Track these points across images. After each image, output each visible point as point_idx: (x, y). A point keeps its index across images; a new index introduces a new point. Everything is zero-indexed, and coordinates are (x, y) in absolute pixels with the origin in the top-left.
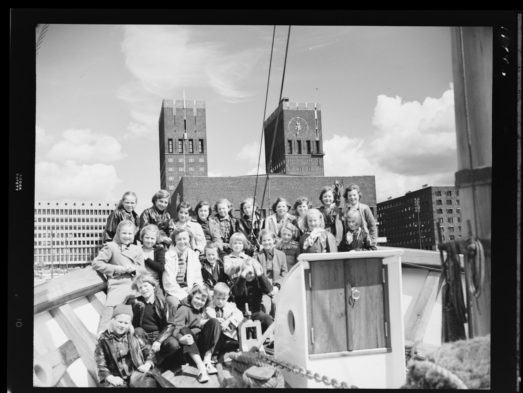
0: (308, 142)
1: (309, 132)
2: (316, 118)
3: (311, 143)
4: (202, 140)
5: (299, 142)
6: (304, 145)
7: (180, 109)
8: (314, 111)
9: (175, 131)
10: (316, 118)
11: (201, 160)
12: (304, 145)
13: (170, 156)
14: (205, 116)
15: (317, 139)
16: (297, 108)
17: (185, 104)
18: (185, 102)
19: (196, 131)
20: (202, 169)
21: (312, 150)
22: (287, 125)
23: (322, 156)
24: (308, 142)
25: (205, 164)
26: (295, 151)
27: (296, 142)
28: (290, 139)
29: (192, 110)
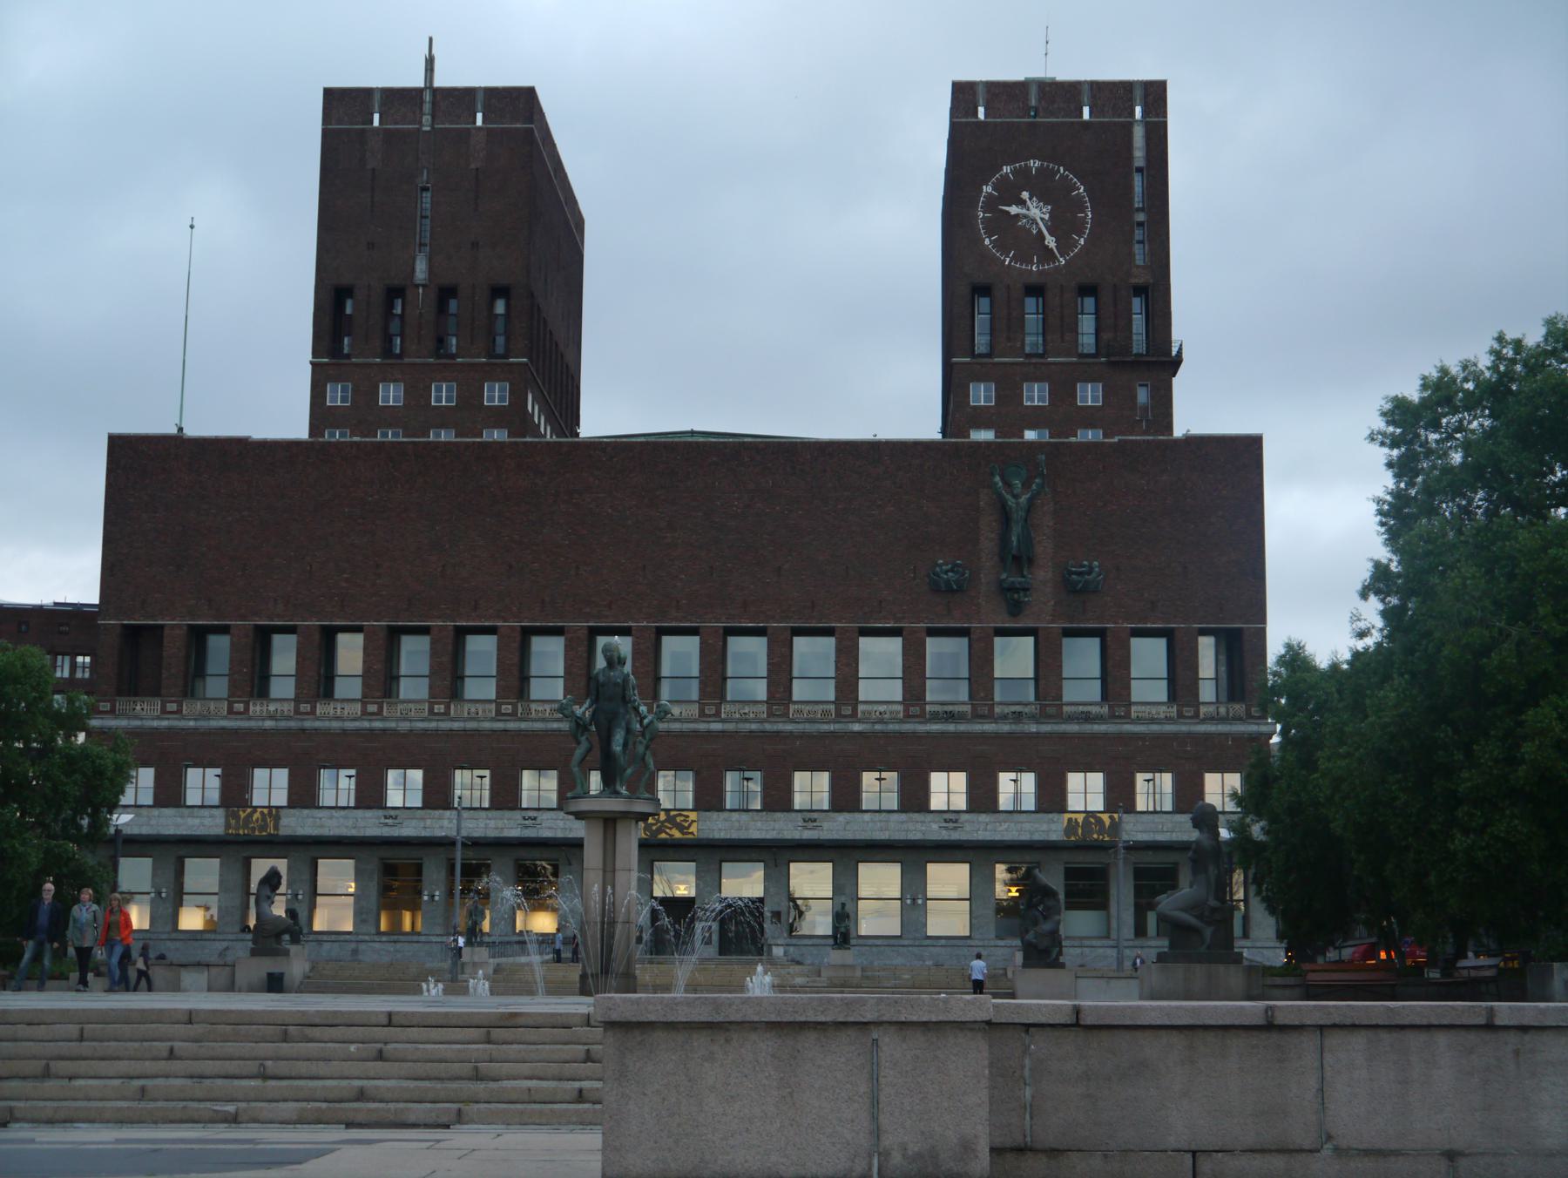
8: (1128, 128)
9: (371, 246)
15: (1139, 279)
17: (427, 107)
18: (427, 97)
19: (475, 245)
21: (1106, 336)
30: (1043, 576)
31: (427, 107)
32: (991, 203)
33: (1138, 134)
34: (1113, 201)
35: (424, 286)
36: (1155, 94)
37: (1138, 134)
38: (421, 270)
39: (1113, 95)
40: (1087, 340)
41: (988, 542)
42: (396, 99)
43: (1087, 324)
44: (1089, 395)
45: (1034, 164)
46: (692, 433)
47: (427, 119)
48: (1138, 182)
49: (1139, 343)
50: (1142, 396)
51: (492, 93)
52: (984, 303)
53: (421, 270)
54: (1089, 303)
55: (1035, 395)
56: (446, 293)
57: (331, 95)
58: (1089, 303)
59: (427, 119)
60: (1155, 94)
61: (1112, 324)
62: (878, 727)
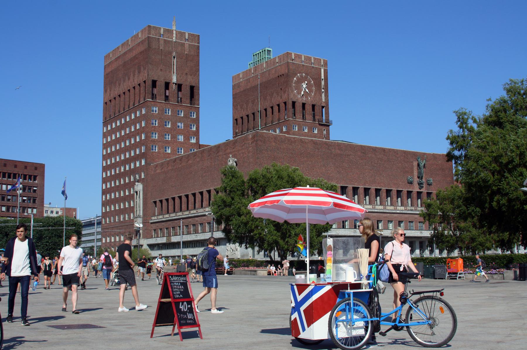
0: (313, 106)
1: (315, 94)
2: (323, 77)
3: (316, 108)
4: (192, 88)
5: (304, 105)
6: (308, 108)
7: (169, 41)
9: (161, 70)
10: (323, 77)
12: (308, 108)
13: (153, 103)
14: (198, 55)
17: (174, 35)
18: (174, 32)
21: (317, 117)
22: (292, 82)
23: (328, 126)
24: (313, 106)
25: (197, 121)
26: (299, 115)
27: (301, 105)
28: (294, 100)
29: (183, 45)
30: (424, 180)
31: (174, 35)
32: (296, 83)
33: (322, 71)
35: (176, 84)
37: (322, 71)
38: (174, 80)
41: (416, 173)
45: (304, 74)
47: (174, 38)
48: (323, 83)
50: (325, 132)
53: (174, 80)
56: (179, 87)
59: (174, 38)
62: (401, 212)
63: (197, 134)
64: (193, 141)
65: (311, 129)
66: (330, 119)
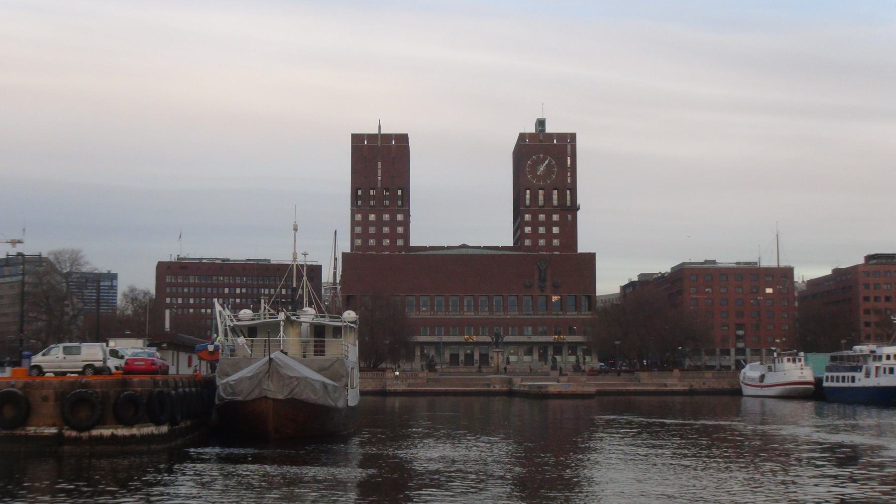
8: (566, 146)
11: (400, 217)
16: (541, 141)
20: (400, 230)
33: (569, 147)
34: (562, 163)
36: (573, 136)
37: (569, 147)
38: (379, 185)
39: (562, 137)
40: (555, 202)
42: (371, 137)
43: (555, 197)
44: (555, 217)
46: (464, 246)
49: (569, 203)
51: (396, 135)
52: (528, 191)
54: (556, 191)
55: (542, 217)
57: (353, 135)
58: (556, 191)
60: (573, 136)
61: (562, 197)
63: (406, 236)
64: (400, 242)
65: (549, 217)
66: (578, 202)
